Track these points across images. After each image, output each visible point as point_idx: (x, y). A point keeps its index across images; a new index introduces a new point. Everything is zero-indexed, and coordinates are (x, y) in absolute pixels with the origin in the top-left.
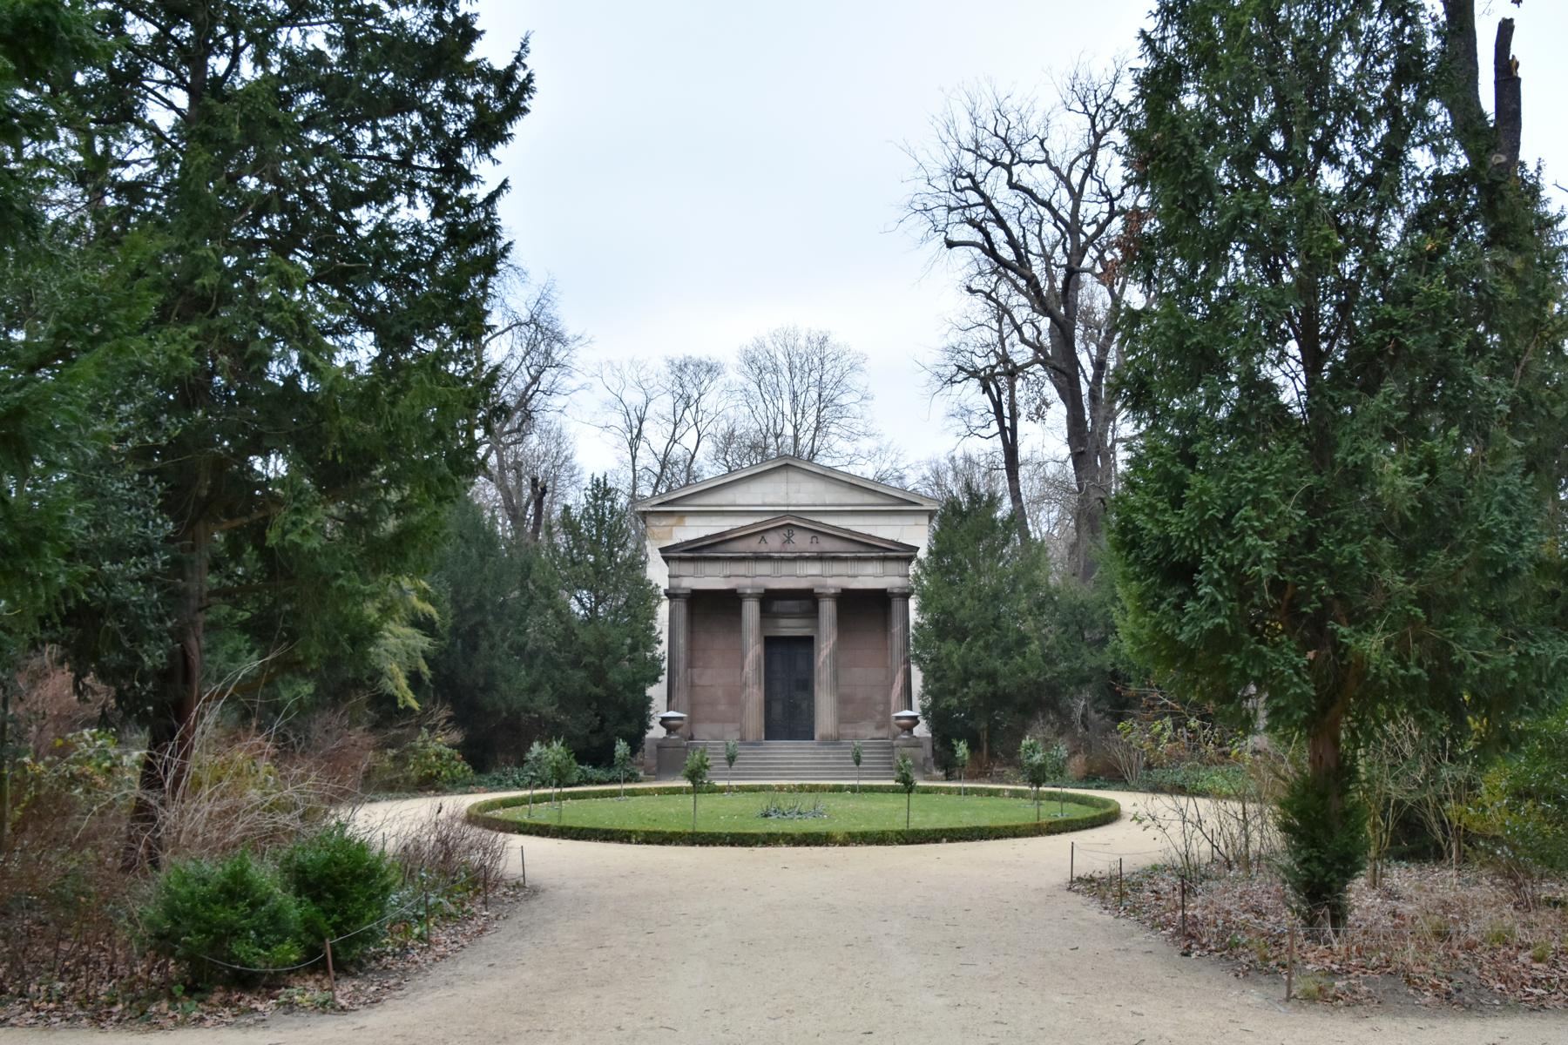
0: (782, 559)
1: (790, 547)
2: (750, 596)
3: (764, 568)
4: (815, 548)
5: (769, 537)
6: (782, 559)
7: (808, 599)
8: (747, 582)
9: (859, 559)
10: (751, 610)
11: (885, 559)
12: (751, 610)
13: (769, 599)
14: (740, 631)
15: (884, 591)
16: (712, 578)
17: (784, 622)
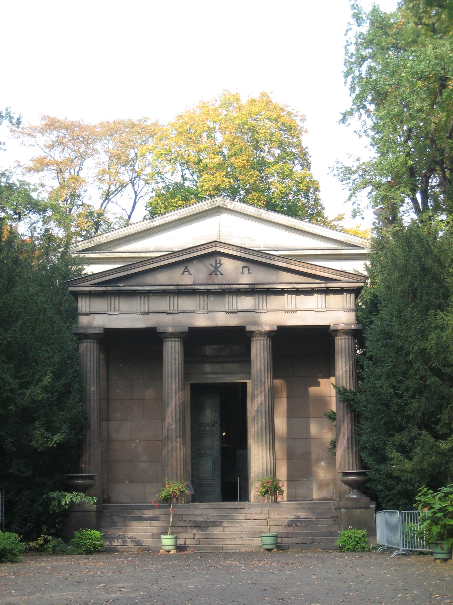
0: (208, 293)
1: (218, 279)
2: (173, 335)
3: (187, 303)
4: (245, 280)
5: (192, 268)
6: (208, 293)
7: (236, 340)
8: (167, 319)
9: (298, 292)
10: (172, 352)
11: (327, 291)
12: (172, 352)
13: (196, 340)
14: (162, 378)
15: (326, 328)
16: (127, 316)
17: (208, 368)
